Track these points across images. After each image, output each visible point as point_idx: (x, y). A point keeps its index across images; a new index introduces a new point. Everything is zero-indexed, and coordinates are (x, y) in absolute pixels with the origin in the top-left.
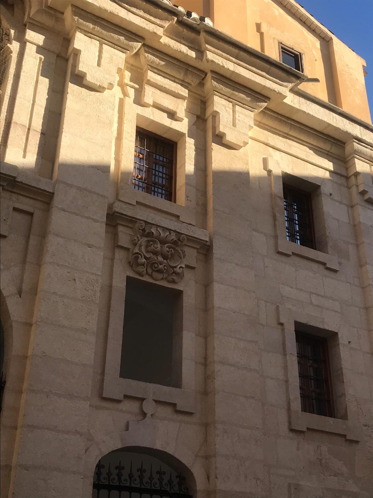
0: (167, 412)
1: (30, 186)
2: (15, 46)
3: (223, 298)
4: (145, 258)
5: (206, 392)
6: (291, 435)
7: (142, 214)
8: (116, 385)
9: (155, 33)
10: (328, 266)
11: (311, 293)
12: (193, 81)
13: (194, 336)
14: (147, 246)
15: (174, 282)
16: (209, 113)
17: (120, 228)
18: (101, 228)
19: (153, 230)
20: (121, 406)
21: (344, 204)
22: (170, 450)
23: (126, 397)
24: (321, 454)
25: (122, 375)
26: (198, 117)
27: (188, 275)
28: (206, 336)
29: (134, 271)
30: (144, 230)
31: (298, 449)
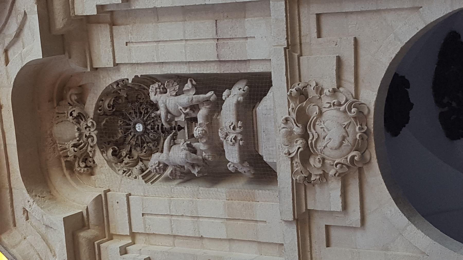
1: (287, 28)
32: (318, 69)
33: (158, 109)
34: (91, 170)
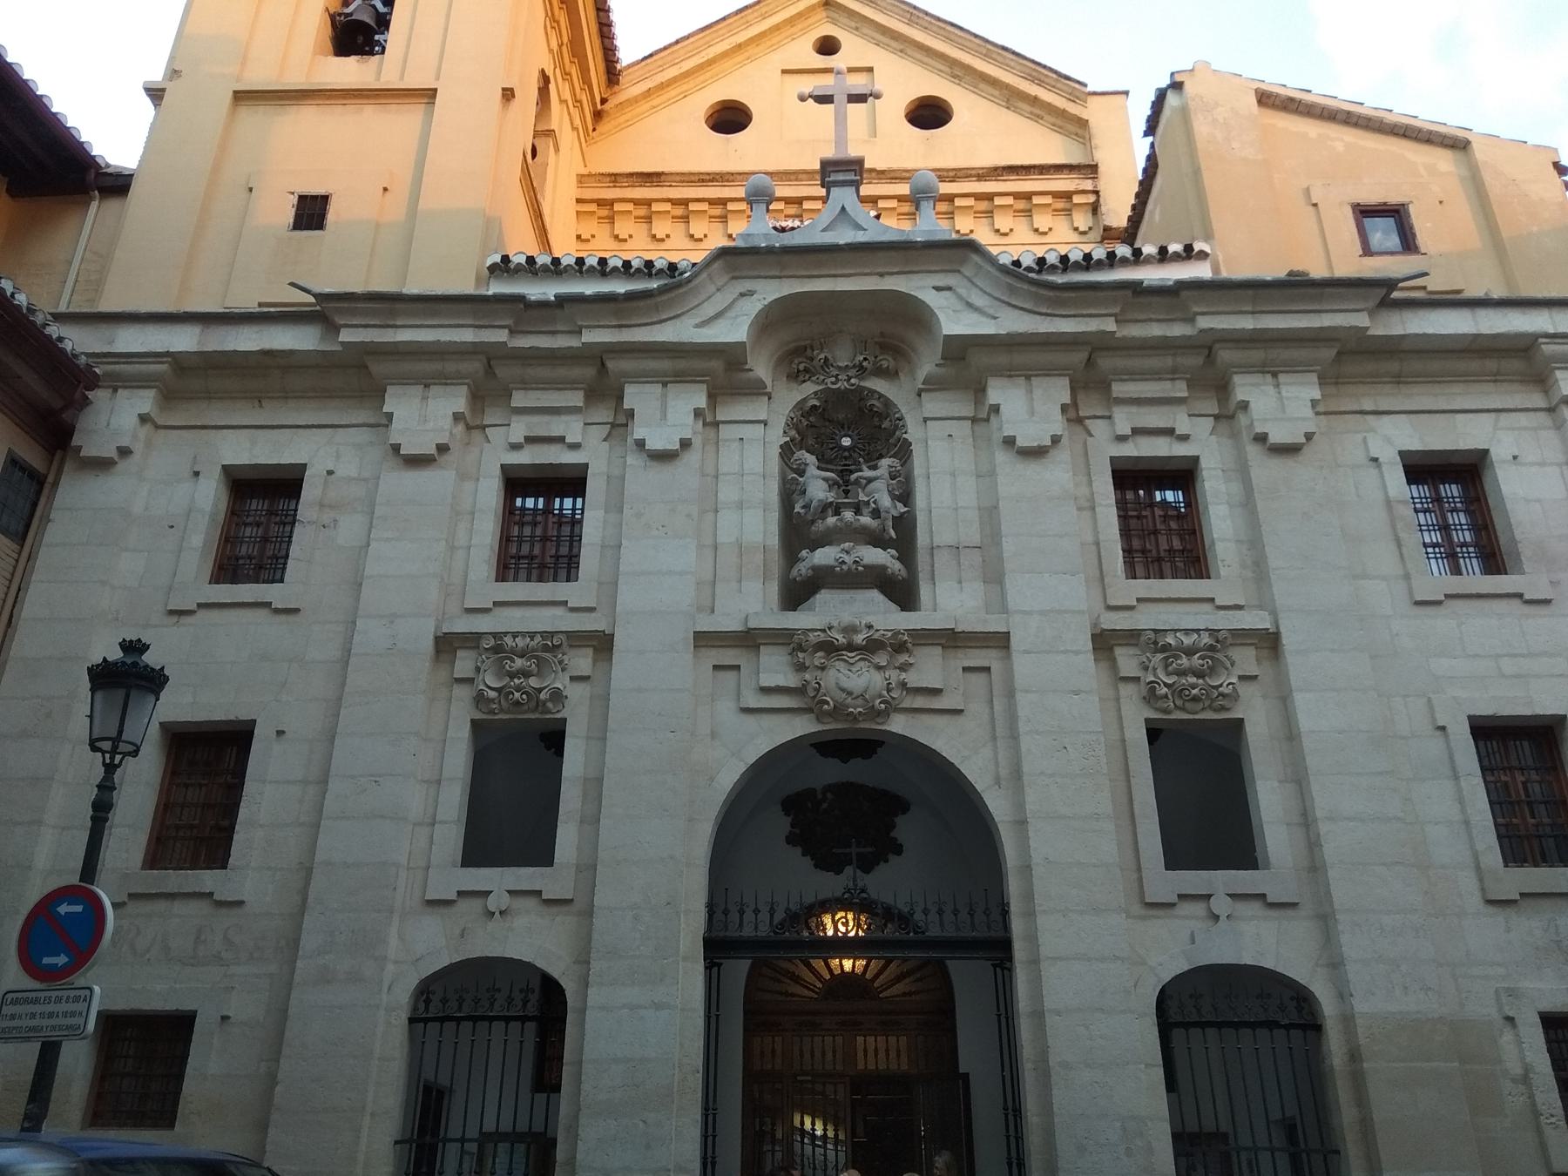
0: (1255, 908)
2: (913, 432)
3: (1310, 713)
4: (1166, 685)
5: (1315, 867)
6: (1491, 909)
7: (1145, 619)
8: (1165, 883)
9: (1104, 332)
10: (1527, 597)
11: (1499, 656)
12: (1194, 361)
13: (1276, 784)
14: (1166, 666)
15: (1223, 708)
16: (1232, 406)
17: (1118, 651)
18: (1087, 660)
19: (1170, 640)
20: (1179, 911)
21: (1552, 464)
22: (1268, 963)
23: (1182, 897)
24: (1557, 934)
25: (1170, 866)
26: (1217, 417)
27: (1245, 690)
28: (1298, 779)
29: (1157, 709)
30: (1156, 643)
31: (1508, 930)
32: (928, 668)
33: (870, 468)
34: (796, 377)
